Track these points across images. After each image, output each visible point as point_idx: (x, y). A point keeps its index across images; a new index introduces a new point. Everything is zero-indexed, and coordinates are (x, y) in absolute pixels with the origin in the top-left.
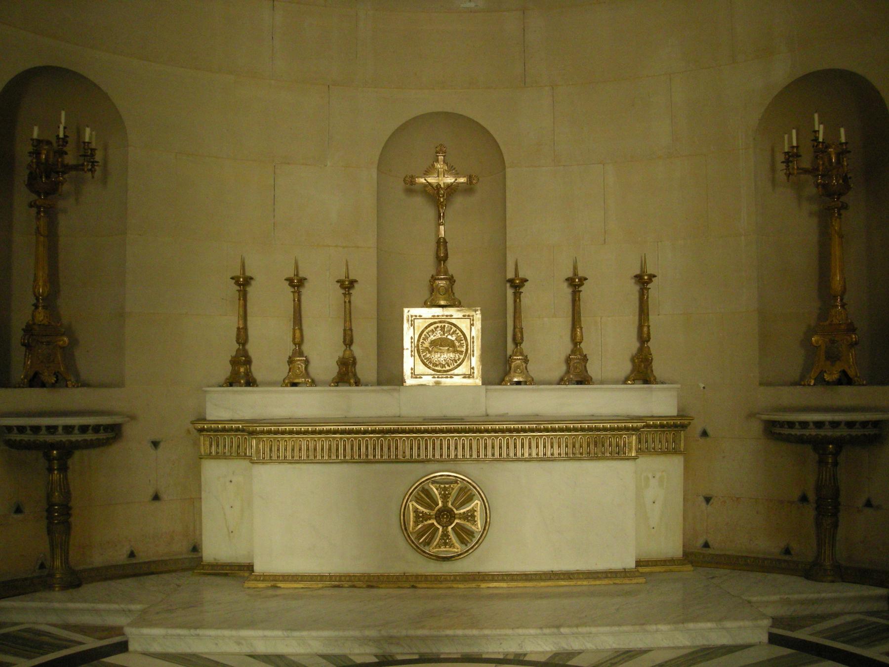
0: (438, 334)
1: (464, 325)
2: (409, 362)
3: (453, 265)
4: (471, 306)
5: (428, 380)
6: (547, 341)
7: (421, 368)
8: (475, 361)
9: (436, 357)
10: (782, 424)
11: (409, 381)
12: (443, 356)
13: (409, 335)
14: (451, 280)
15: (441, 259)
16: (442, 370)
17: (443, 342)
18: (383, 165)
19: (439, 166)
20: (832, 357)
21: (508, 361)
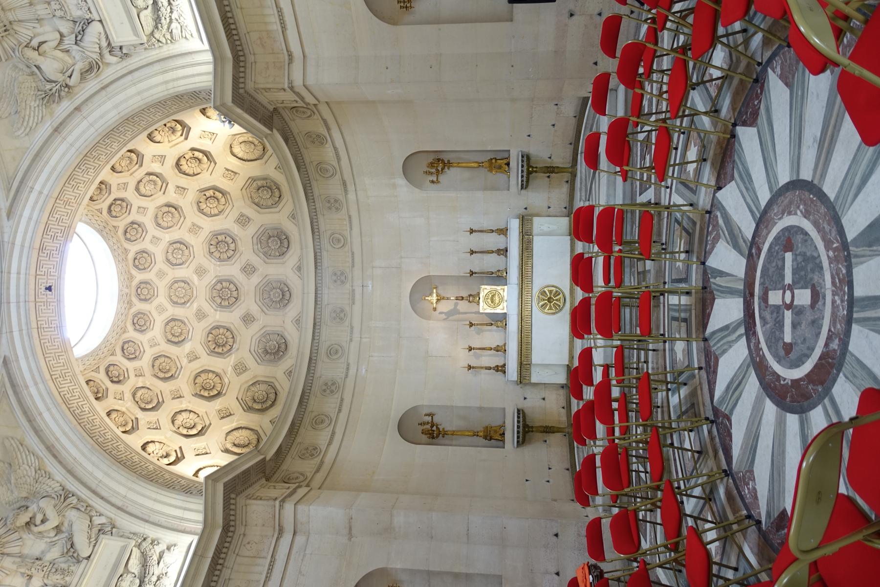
0: (489, 300)
1: (486, 292)
2: (498, 310)
3: (465, 295)
4: (479, 289)
5: (505, 304)
6: (492, 262)
7: (501, 307)
8: (499, 288)
9: (497, 301)
10: (522, 185)
11: (505, 311)
12: (497, 299)
13: (489, 310)
14: (470, 296)
15: (463, 298)
16: (502, 299)
17: (492, 299)
18: (428, 318)
19: (429, 298)
20: (500, 167)
21: (498, 276)
